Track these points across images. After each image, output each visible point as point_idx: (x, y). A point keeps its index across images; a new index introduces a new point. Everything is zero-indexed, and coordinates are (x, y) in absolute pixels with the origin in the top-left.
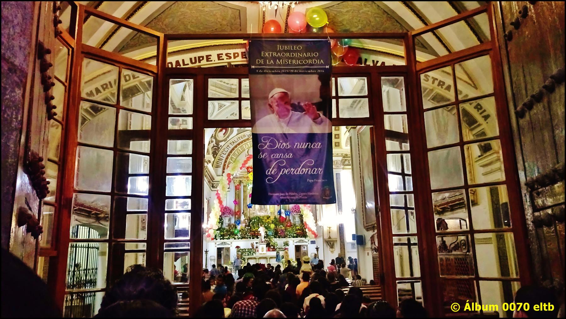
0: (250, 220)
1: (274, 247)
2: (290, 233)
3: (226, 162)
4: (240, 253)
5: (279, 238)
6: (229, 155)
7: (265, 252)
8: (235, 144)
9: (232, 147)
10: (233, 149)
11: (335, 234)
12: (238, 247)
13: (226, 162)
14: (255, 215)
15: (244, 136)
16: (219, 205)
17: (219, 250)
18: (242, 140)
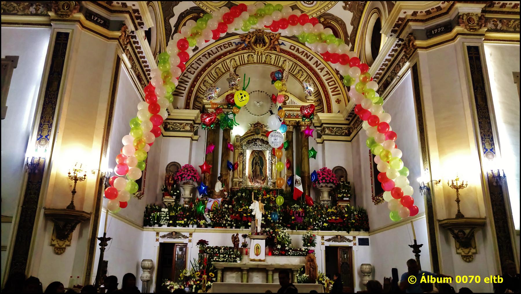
0: (233, 193)
1: (283, 246)
2: (315, 220)
3: (193, 86)
4: (206, 256)
5: (293, 228)
6: (200, 74)
7: (262, 256)
8: (212, 57)
9: (206, 61)
10: (208, 65)
11: (478, 206)
12: (202, 243)
13: (193, 86)
14: (243, 186)
15: (230, 44)
16: (149, 115)
17: (166, 250)
18: (225, 50)
